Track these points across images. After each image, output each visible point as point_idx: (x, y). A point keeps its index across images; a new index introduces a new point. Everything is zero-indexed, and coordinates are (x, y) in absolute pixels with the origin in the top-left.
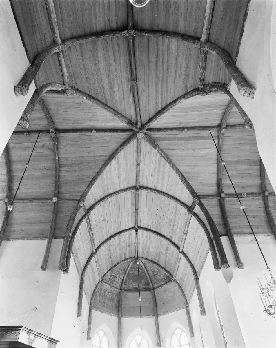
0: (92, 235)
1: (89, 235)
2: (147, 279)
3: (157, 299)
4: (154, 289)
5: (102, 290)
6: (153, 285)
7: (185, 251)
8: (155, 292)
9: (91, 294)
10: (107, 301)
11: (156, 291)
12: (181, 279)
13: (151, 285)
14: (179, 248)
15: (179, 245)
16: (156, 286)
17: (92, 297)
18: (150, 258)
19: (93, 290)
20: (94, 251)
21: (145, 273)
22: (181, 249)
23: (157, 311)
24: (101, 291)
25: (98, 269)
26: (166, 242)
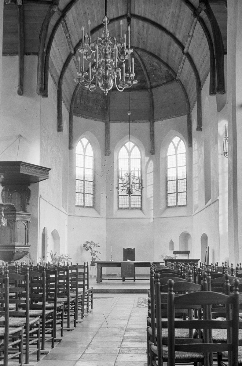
0: (70, 37)
1: (65, 37)
2: (143, 74)
3: (155, 100)
4: (152, 87)
5: (84, 91)
6: (150, 83)
7: (190, 52)
8: (153, 92)
9: (69, 100)
10: (91, 104)
11: (154, 90)
12: (185, 81)
13: (148, 82)
14: (183, 48)
15: (184, 44)
16: (154, 84)
17: (72, 101)
18: (148, 49)
19: (72, 93)
20: (73, 52)
21: (140, 67)
22: (185, 50)
23: (153, 115)
24: (82, 92)
25: (77, 69)
26: (167, 38)
